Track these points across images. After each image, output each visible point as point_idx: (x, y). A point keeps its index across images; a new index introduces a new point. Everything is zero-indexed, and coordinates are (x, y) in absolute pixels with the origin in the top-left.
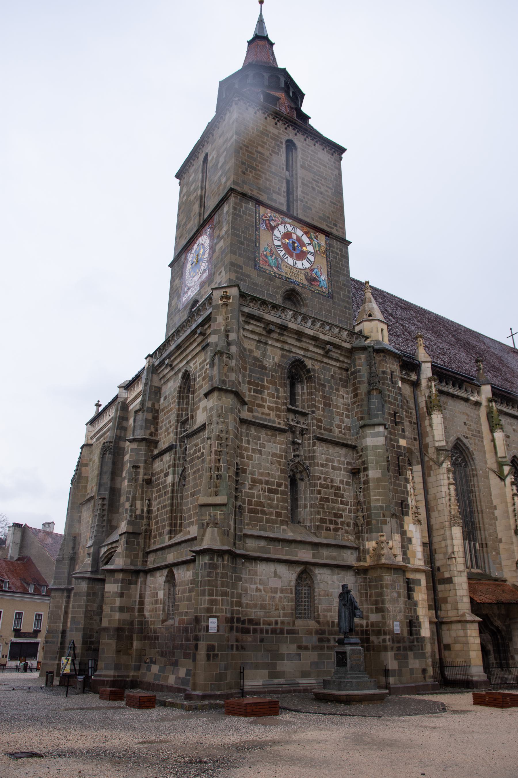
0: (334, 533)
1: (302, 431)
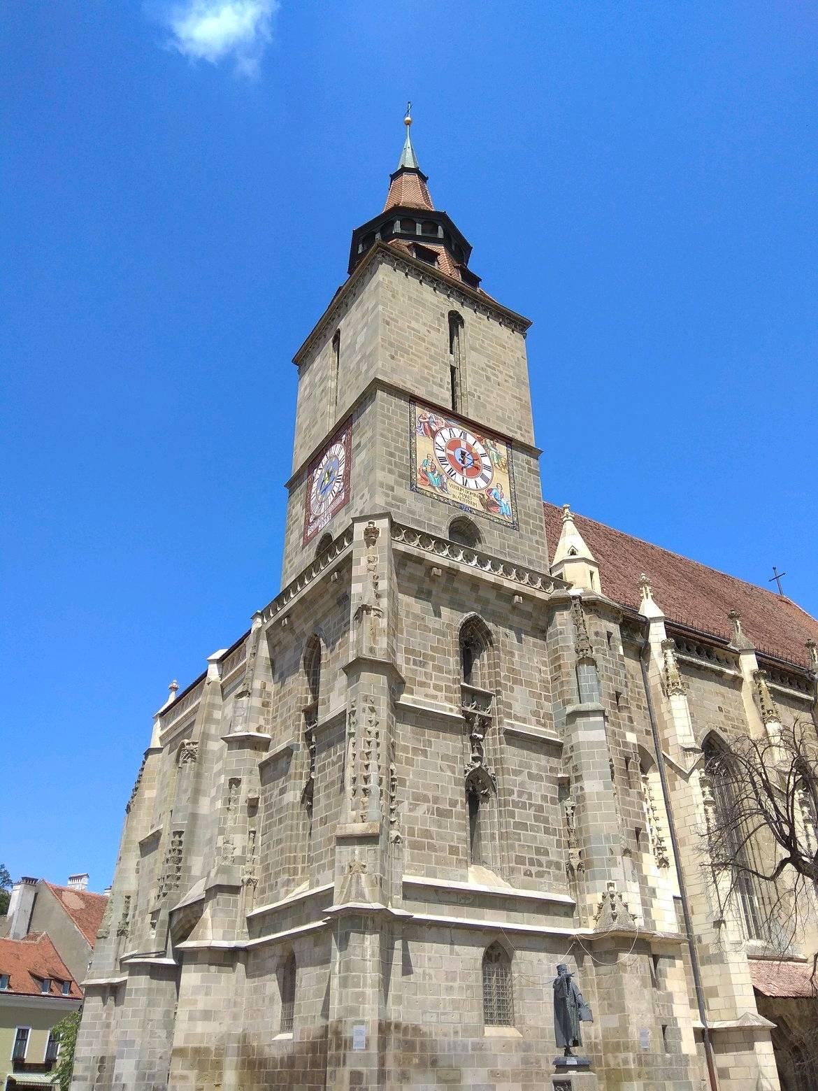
0: (538, 879)
1: (484, 722)
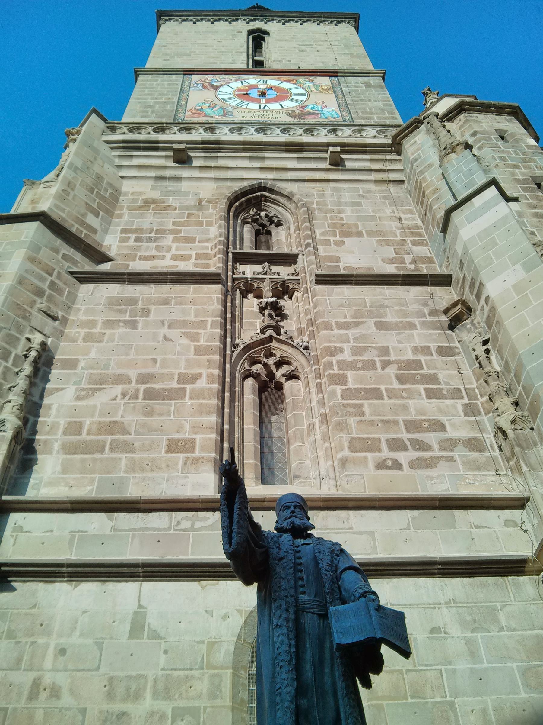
0: (419, 472)
